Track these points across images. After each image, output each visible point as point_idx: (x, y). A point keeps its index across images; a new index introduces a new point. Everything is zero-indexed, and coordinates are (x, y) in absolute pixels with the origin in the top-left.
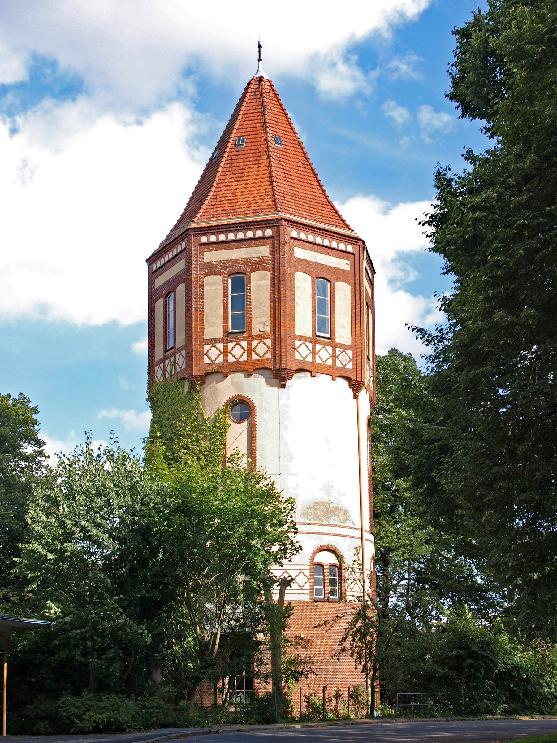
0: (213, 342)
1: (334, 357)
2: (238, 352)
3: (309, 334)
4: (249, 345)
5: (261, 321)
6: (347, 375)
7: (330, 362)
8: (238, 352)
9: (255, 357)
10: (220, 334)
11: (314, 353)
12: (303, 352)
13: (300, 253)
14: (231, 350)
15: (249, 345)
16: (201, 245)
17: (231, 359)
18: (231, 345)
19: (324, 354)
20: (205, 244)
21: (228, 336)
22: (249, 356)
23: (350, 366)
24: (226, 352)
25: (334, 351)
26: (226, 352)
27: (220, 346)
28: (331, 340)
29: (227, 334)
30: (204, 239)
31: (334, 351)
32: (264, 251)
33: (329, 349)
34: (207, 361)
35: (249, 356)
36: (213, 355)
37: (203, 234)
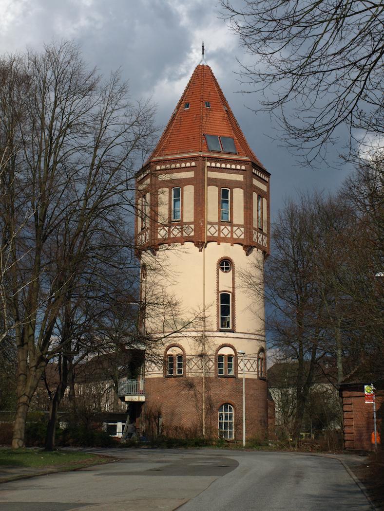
1: (232, 232)
3: (216, 220)
5: (189, 216)
6: (242, 243)
7: (229, 236)
11: (219, 231)
12: (212, 231)
13: (212, 175)
19: (226, 231)
21: (170, 224)
23: (242, 237)
24: (169, 232)
25: (232, 229)
26: (169, 232)
28: (231, 223)
30: (158, 168)
31: (232, 229)
32: (190, 174)
33: (229, 228)
34: (159, 237)
36: (162, 233)
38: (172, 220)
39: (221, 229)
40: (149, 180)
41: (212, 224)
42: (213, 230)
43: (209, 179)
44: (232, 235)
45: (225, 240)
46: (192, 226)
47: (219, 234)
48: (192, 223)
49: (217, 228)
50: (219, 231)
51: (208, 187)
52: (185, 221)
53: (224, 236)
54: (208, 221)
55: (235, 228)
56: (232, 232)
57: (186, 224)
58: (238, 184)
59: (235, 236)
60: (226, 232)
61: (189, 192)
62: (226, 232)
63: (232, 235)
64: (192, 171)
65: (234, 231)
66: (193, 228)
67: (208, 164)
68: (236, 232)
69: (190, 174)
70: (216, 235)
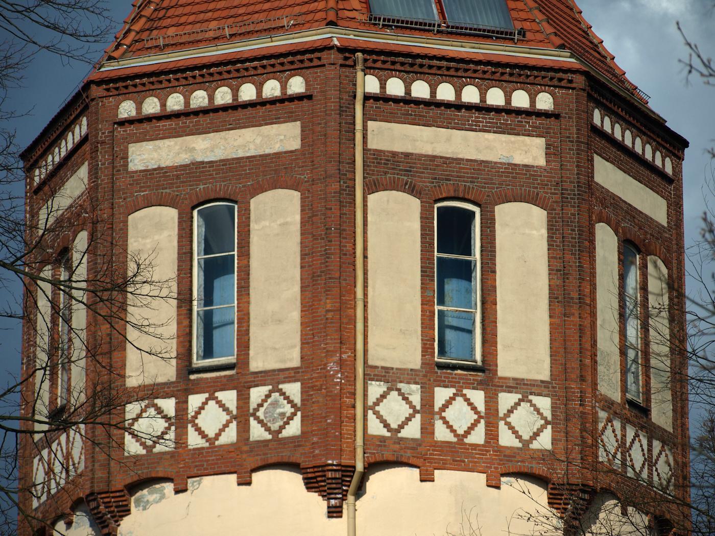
0: (151, 393)
2: (213, 418)
4: (243, 399)
5: (276, 333)
8: (213, 418)
9: (257, 432)
10: (167, 372)
11: (428, 412)
12: (391, 412)
14: (195, 417)
15: (243, 399)
16: (123, 123)
17: (194, 440)
18: (195, 401)
19: (460, 414)
20: (130, 122)
22: (244, 429)
25: (492, 402)
26: (181, 421)
27: (169, 405)
28: (484, 373)
29: (186, 368)
30: (127, 109)
31: (492, 402)
32: (284, 137)
33: (478, 397)
35: (244, 429)
37: (125, 94)
38: (197, 362)
39: (439, 402)
40: (83, 172)
41: (391, 377)
42: (394, 409)
43: (375, 158)
44: (492, 434)
45: (457, 456)
46: (294, 389)
47: (427, 429)
48: (289, 375)
49: (416, 399)
50: (428, 412)
51: (372, 198)
52: (257, 364)
53: (450, 437)
54: (370, 362)
55: (506, 400)
56: (491, 417)
57: (263, 377)
58: (515, 184)
59: (506, 439)
60: (460, 415)
61: (276, 223)
62: (460, 415)
63: (492, 434)
64: (290, 118)
65: (502, 411)
66: (297, 400)
67: (372, 84)
68: (512, 419)
69: (284, 137)
70: (413, 431)
